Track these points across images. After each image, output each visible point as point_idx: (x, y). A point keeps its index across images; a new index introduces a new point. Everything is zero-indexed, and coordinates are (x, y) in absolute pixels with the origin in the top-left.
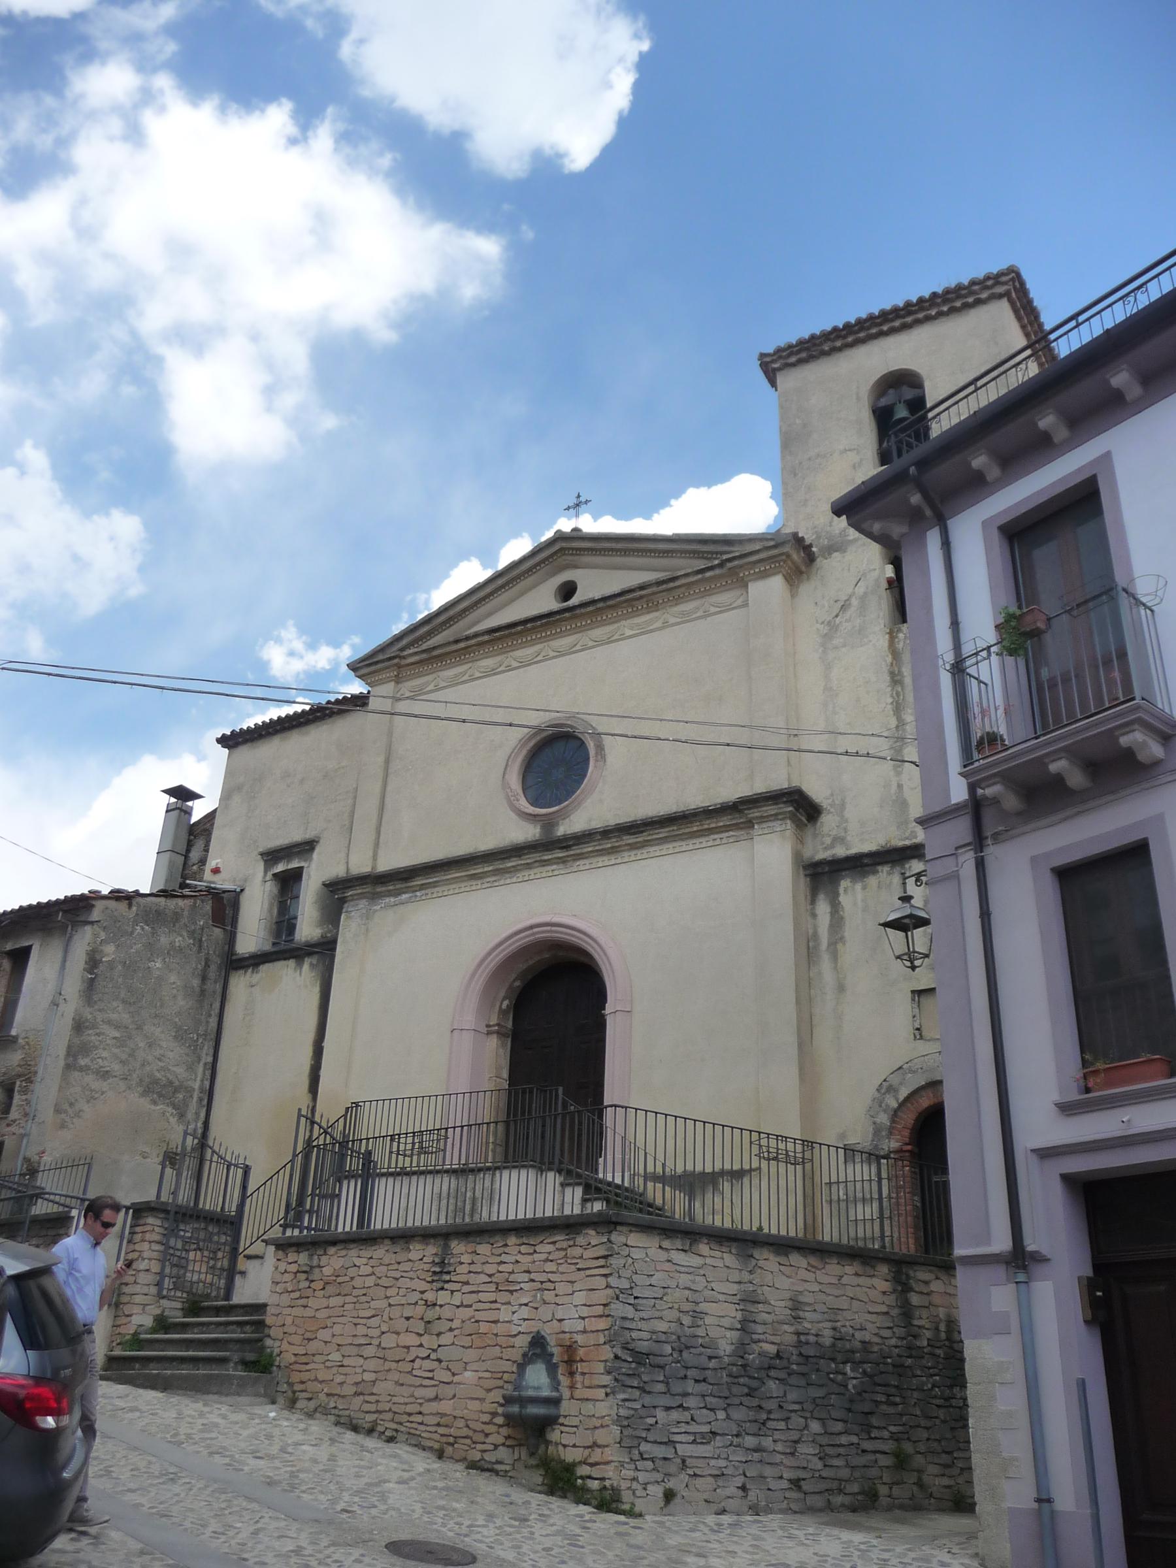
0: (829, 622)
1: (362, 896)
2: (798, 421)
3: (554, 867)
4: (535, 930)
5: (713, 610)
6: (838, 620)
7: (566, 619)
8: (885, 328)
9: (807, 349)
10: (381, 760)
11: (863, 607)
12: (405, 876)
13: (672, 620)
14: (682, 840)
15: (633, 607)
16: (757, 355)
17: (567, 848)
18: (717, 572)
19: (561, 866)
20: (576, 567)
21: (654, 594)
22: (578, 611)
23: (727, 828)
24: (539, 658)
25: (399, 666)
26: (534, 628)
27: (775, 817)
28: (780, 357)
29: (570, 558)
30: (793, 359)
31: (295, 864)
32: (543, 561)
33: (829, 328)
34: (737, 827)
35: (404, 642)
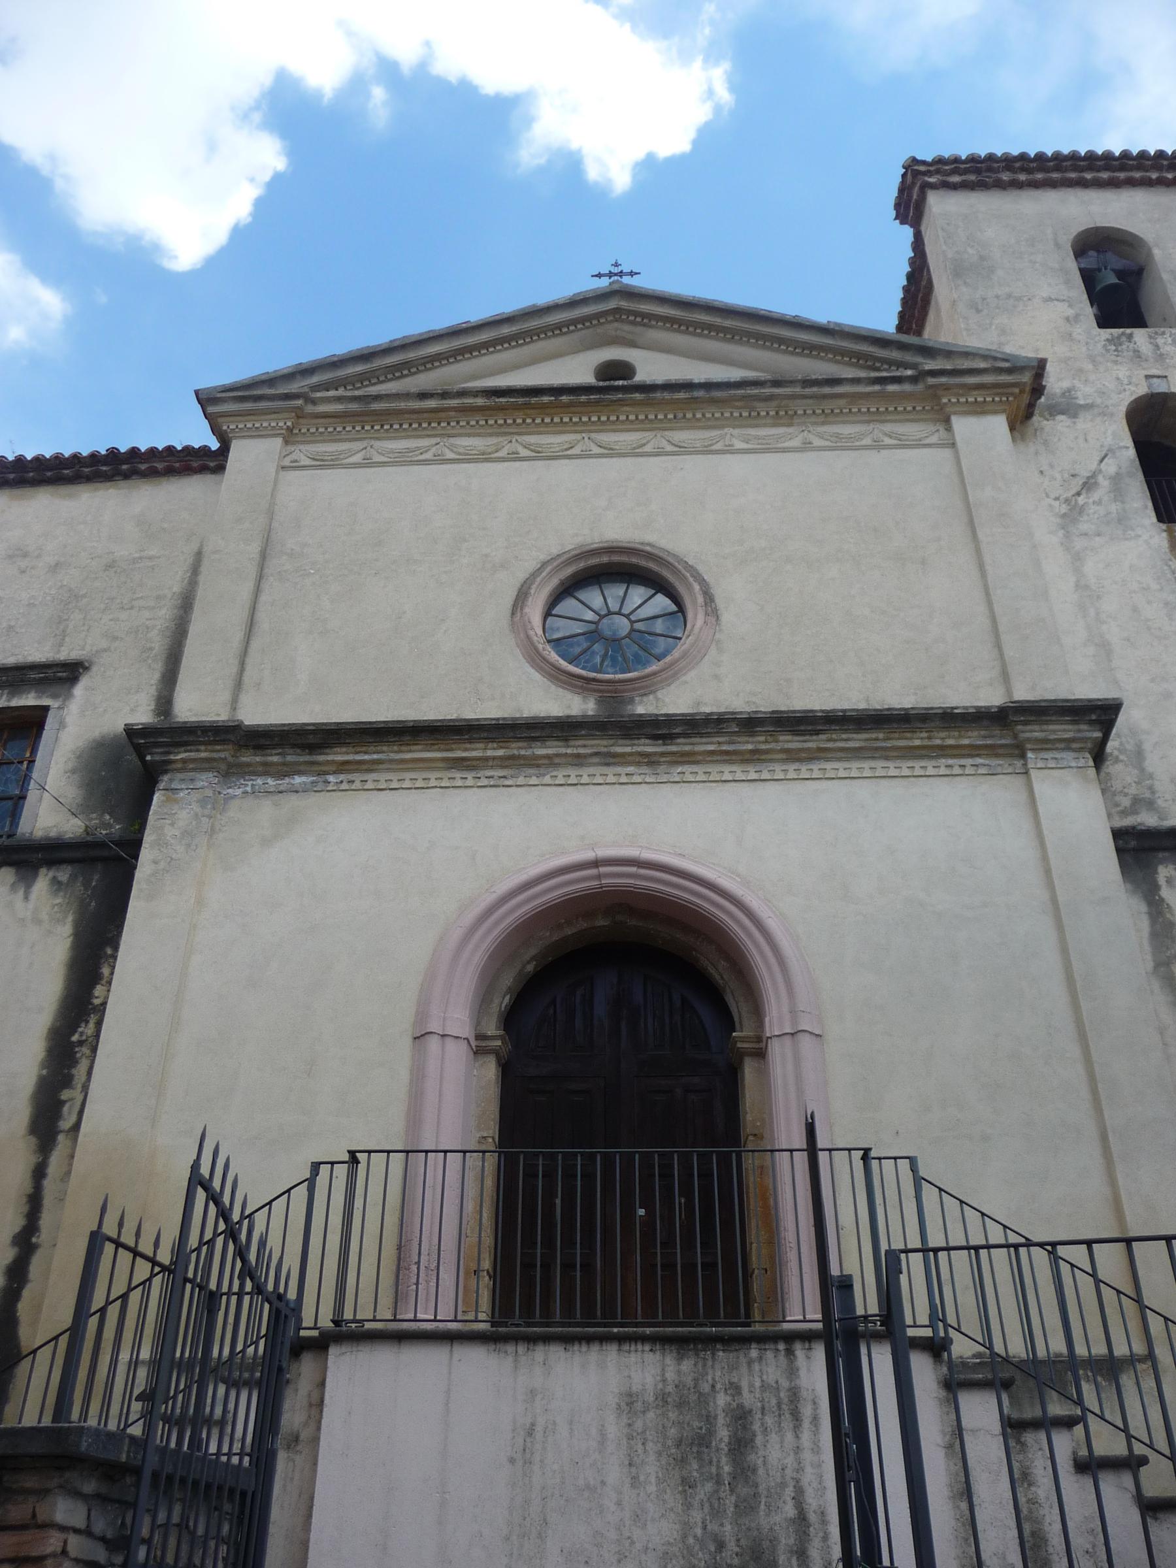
0: (1067, 501)
1: (206, 765)
2: (970, 251)
3: (631, 769)
4: (603, 870)
5: (888, 441)
6: (1081, 500)
7: (634, 403)
8: (1088, 176)
9: (978, 171)
10: (254, 548)
11: (1118, 492)
12: (311, 739)
13: (817, 442)
14: (887, 758)
15: (752, 409)
16: (904, 158)
17: (667, 738)
18: (907, 387)
19: (645, 770)
20: (633, 344)
21: (793, 397)
22: (658, 395)
23: (973, 751)
24: (569, 452)
25: (300, 414)
26: (571, 405)
27: (1067, 744)
28: (938, 172)
29: (627, 327)
30: (956, 179)
31: (29, 700)
32: (583, 320)
33: (1015, 152)
34: (992, 751)
35: (315, 379)
